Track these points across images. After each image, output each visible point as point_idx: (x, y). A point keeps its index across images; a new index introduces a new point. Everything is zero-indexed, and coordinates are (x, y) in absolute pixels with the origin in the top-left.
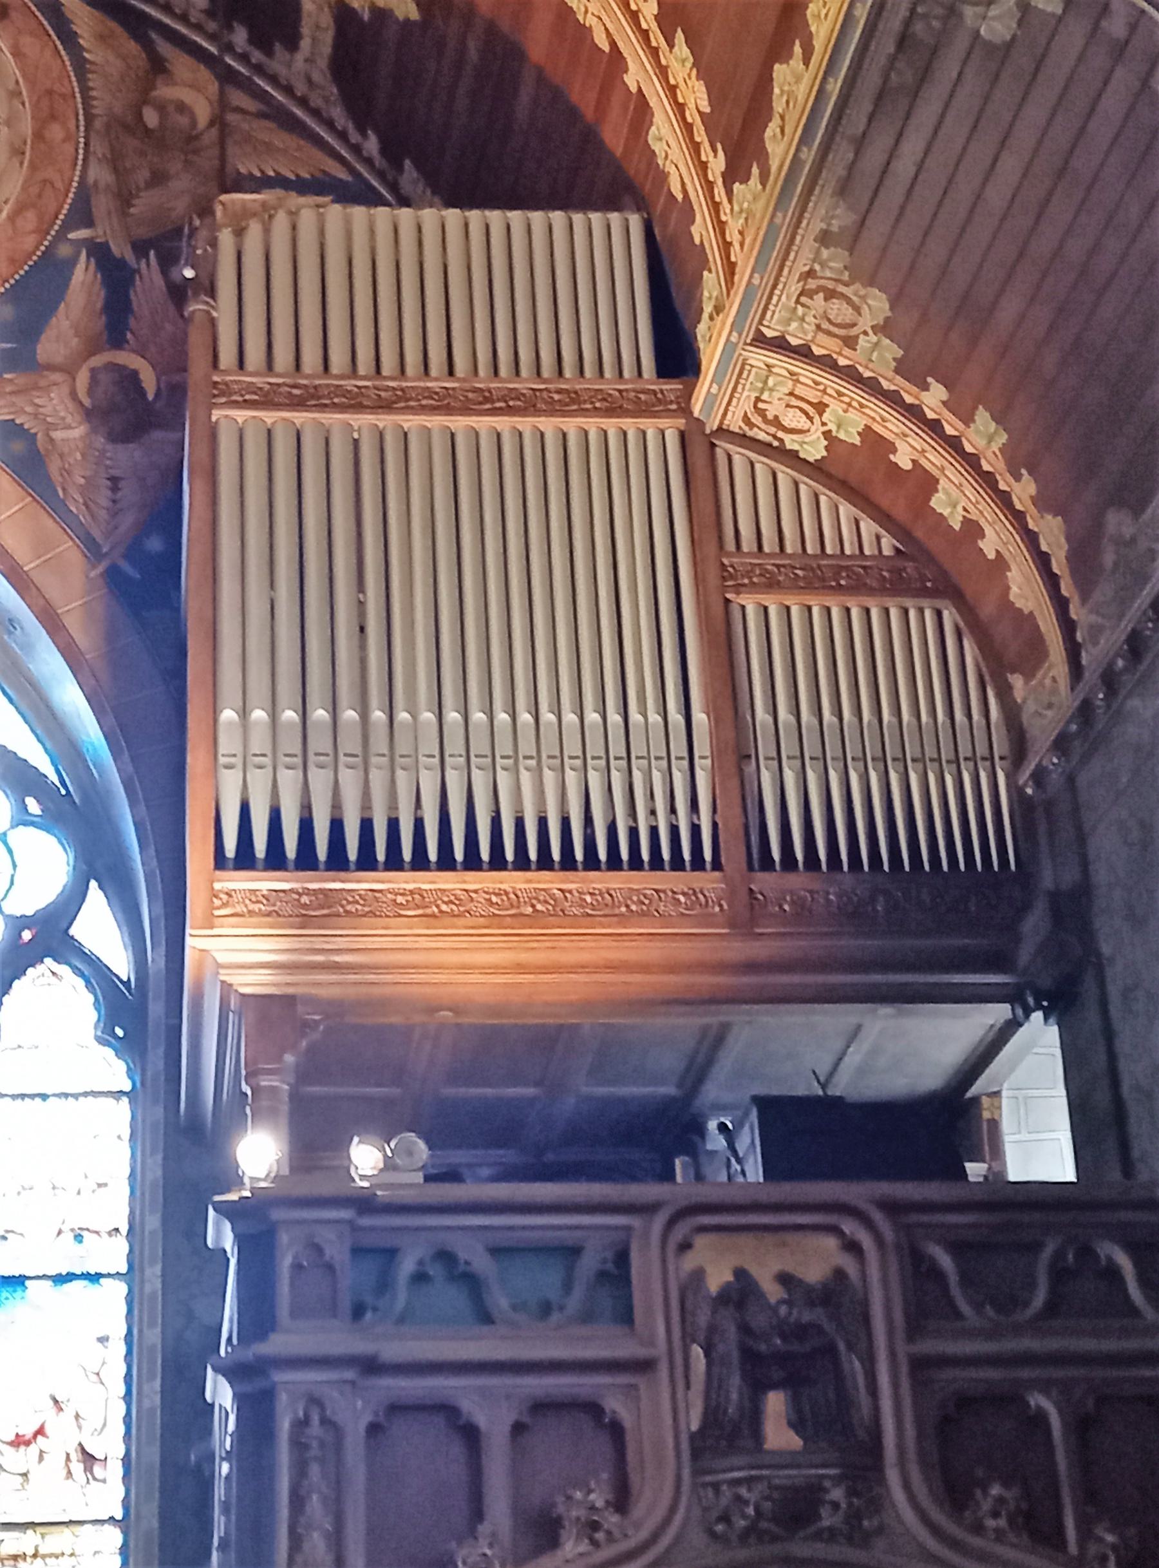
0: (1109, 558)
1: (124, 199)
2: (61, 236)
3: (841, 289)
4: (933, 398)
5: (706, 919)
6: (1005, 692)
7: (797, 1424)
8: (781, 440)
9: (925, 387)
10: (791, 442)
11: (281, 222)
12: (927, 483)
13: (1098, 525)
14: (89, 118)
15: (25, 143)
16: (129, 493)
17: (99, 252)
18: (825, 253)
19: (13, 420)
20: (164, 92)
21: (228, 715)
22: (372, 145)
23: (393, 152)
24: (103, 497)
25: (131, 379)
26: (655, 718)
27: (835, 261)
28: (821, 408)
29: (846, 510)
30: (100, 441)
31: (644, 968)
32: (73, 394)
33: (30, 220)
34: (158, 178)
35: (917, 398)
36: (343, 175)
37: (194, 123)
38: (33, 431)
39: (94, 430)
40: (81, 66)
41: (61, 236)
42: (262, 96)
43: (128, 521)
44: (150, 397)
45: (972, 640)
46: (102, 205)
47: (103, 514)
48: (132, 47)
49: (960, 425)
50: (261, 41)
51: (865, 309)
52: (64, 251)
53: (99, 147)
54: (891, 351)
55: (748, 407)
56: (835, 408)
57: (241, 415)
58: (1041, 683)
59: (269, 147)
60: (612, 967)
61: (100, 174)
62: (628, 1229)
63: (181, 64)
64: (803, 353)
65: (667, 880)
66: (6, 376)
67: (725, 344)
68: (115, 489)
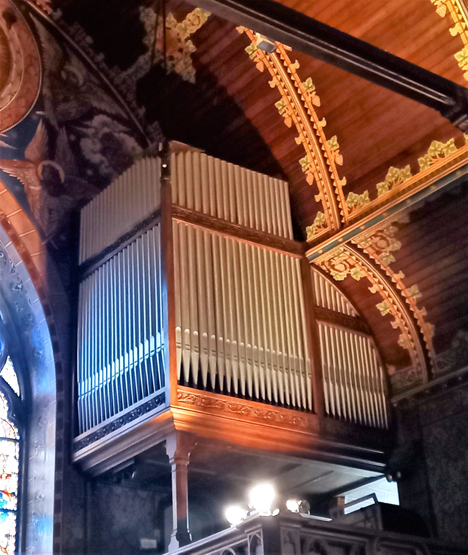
0: (455, 344)
1: (55, 104)
3: (388, 238)
6: (385, 370)
8: (330, 272)
9: (396, 272)
10: (333, 273)
11: (188, 154)
12: (378, 298)
13: (453, 333)
14: (44, 70)
15: (22, 72)
16: (55, 216)
18: (391, 227)
19: (16, 178)
21: (178, 329)
22: (142, 111)
24: (46, 215)
25: (55, 173)
26: (295, 357)
27: (393, 229)
28: (352, 267)
29: (343, 298)
30: (45, 194)
32: (37, 173)
33: (23, 102)
34: (66, 100)
35: (391, 275)
36: (125, 116)
37: (78, 82)
38: (23, 183)
39: (43, 189)
42: (101, 80)
43: (54, 227)
44: (63, 180)
45: (377, 351)
46: (48, 104)
47: (46, 223)
48: (58, 47)
49: (403, 287)
50: (110, 62)
51: (391, 246)
52: (34, 118)
53: (47, 80)
54: (392, 259)
55: (327, 259)
56: (358, 268)
57: (179, 221)
58: (406, 372)
59: (102, 100)
60: (259, 436)
61: (46, 91)
62: (364, 543)
63: (74, 60)
64: (360, 251)
66: (15, 160)
67: (336, 241)
68: (50, 213)
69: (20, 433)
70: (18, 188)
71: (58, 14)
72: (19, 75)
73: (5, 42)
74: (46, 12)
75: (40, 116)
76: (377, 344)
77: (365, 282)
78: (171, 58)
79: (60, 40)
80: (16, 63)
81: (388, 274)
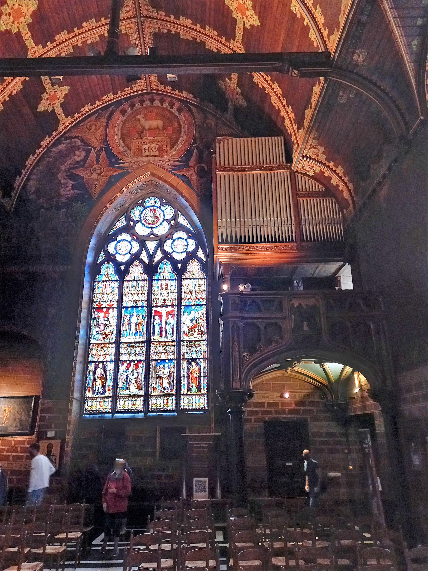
2: (192, 146)
4: (331, 164)
5: (295, 250)
7: (308, 327)
9: (330, 163)
10: (308, 173)
11: (226, 141)
12: (330, 178)
17: (197, 147)
20: (208, 121)
21: (219, 220)
23: (243, 129)
25: (204, 167)
26: (286, 218)
27: (315, 142)
28: (313, 167)
29: (317, 184)
30: (198, 178)
31: (284, 258)
32: (195, 171)
33: (187, 143)
40: (194, 118)
41: (192, 146)
42: (222, 121)
51: (320, 150)
54: (325, 157)
56: (315, 167)
57: (220, 173)
60: (279, 258)
62: (282, 297)
64: (310, 158)
65: (287, 244)
69: (206, 275)
70: (186, 179)
71: (198, 100)
72: (185, 132)
73: (178, 121)
74: (194, 101)
75: (195, 147)
76: (337, 201)
77: (322, 172)
78: (237, 99)
79: (203, 111)
80: (183, 128)
81: (327, 165)
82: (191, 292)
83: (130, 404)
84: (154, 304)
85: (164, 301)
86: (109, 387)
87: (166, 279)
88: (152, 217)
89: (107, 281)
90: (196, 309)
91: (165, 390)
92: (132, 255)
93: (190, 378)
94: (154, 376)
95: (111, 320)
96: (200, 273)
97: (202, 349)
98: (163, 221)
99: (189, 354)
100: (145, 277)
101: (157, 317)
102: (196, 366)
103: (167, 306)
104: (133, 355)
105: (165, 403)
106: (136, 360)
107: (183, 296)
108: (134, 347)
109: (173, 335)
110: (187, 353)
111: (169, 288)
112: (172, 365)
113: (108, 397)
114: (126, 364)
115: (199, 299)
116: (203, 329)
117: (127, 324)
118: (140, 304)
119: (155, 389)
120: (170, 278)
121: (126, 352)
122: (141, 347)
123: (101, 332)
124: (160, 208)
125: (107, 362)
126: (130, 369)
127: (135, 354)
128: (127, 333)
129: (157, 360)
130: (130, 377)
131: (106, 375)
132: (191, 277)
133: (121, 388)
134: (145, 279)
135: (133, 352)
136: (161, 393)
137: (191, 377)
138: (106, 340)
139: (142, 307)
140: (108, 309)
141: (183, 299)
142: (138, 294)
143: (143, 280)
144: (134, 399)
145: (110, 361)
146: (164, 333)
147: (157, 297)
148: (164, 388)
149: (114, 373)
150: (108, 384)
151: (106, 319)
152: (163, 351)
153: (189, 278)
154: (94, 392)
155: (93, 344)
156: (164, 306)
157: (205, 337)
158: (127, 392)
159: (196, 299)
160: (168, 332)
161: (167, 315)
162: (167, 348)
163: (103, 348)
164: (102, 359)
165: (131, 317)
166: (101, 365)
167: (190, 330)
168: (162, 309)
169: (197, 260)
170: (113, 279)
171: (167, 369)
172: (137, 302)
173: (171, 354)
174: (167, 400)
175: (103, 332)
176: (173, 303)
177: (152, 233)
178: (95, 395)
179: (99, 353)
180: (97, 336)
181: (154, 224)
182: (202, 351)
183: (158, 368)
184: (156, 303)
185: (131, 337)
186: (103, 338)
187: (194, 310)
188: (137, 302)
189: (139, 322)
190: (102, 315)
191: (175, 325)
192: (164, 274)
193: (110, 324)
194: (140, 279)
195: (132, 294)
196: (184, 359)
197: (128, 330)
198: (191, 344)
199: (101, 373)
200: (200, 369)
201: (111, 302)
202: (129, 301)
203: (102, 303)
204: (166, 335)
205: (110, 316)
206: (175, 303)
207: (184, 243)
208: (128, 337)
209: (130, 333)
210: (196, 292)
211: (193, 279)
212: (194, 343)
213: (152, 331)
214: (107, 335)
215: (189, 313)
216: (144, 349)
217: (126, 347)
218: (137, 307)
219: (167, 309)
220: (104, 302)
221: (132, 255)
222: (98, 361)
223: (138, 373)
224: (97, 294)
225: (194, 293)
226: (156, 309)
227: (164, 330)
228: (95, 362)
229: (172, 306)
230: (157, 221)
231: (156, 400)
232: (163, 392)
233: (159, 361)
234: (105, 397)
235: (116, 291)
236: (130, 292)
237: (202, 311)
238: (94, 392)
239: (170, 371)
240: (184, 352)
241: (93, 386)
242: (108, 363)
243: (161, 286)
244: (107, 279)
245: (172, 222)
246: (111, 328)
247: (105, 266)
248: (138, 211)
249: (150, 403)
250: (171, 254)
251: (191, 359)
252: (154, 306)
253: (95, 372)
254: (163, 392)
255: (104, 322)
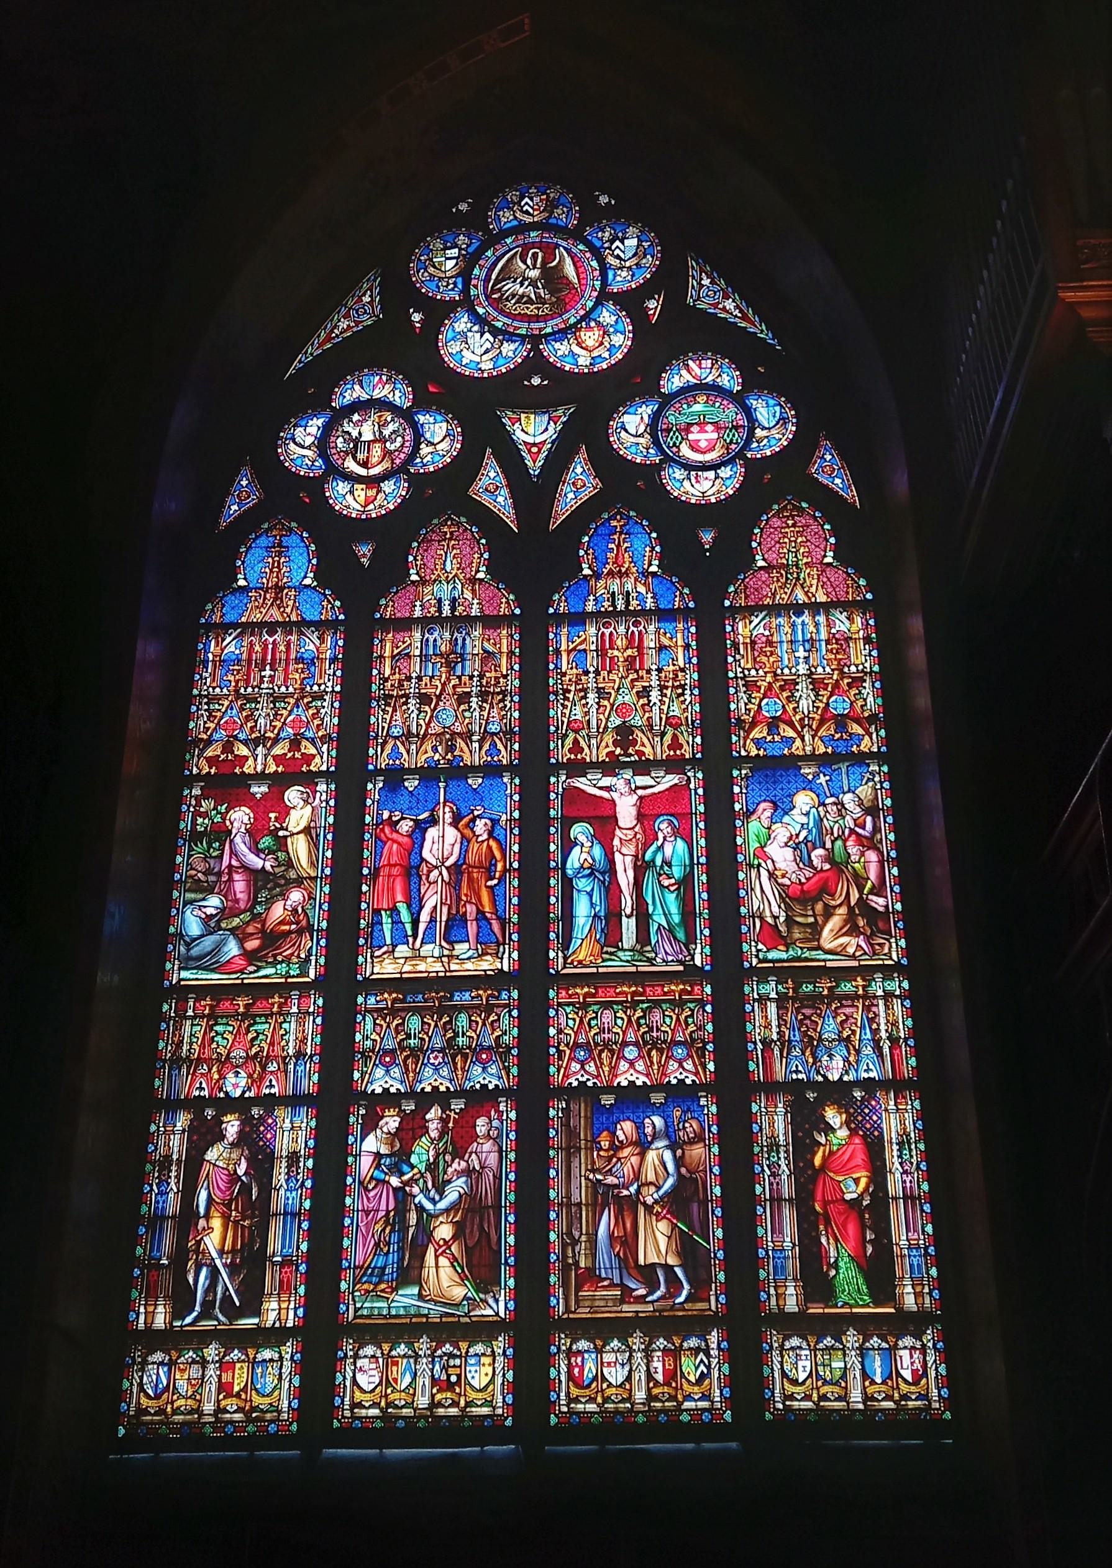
82: (790, 685)
83: (424, 1381)
84: (561, 752)
85: (625, 735)
86: (287, 1262)
87: (627, 613)
88: (533, 283)
89: (272, 627)
90: (822, 779)
91: (653, 1286)
92: (418, 482)
93: (818, 1208)
94: (580, 1194)
95: (300, 847)
96: (837, 576)
97: (883, 1021)
98: (599, 303)
99: (796, 1052)
100: (506, 604)
101: (580, 831)
102: (853, 1132)
103: (643, 767)
104: (435, 1059)
105: (660, 1377)
106: (460, 1093)
107: (740, 705)
108: (441, 1011)
109: (691, 938)
110: (786, 1044)
111: (651, 660)
112: (692, 1127)
113: (275, 1336)
114: (391, 1122)
115: (841, 722)
116: (878, 902)
117: (395, 871)
118: (472, 754)
119: (591, 1276)
120: (649, 604)
121: (390, 1044)
122: (489, 1009)
123: (236, 921)
124: (576, 235)
125: (270, 1102)
126: (422, 1153)
127: (451, 1050)
128: (397, 922)
129: (597, 1091)
130: (420, 1198)
131: (267, 1188)
132: (782, 598)
133: (362, 1271)
134: (504, 610)
135: (438, 1042)
136: (629, 1309)
137: (825, 1204)
138: (270, 971)
139: (491, 771)
140: (279, 782)
141: (740, 721)
142: (464, 698)
143: (491, 622)
144: (448, 1348)
145: (294, 1101)
146: (629, 927)
147: (578, 713)
148: (648, 1274)
149: (314, 1173)
150: (275, 1244)
151: (266, 842)
152: (631, 1037)
153: (768, 601)
154: (182, 1301)
155: (182, 992)
156: (626, 765)
157: (894, 949)
158: (405, 1299)
159: (822, 722)
160: (659, 918)
161: (640, 817)
162: (656, 1016)
163: (249, 1016)
164: (236, 1084)
165: (421, 828)
166: (232, 1127)
167: (798, 908)
168: (606, 781)
169: (814, 506)
170: (311, 615)
171: (659, 1155)
172: (460, 743)
173: (680, 1052)
174: (674, 1354)
175: (246, 917)
176: (675, 744)
177: (536, 362)
178: (188, 1320)
179: (222, 1045)
180: (209, 942)
181: (545, 319)
182: (884, 1035)
183: (605, 1144)
184: (576, 748)
185: (427, 949)
186: (250, 957)
187: (809, 785)
188: (460, 743)
189: (471, 858)
190: (240, 817)
191: (701, 878)
192: (615, 585)
193: (292, 875)
194: (475, 611)
195: (424, 699)
196: (771, 1088)
197: (402, 908)
198: (807, 988)
199: (233, 1178)
200: (875, 1148)
201: (295, 744)
202: (408, 735)
203: (243, 751)
204: (643, 935)
205: (299, 818)
206: (691, 744)
207: (730, 413)
208: (402, 950)
209: (415, 923)
210: (817, 685)
211: (798, 609)
212: (824, 986)
213: (556, 911)
214: (272, 939)
215: (781, 808)
216: (508, 1028)
217: (393, 1012)
218: (458, 772)
219: (641, 780)
220: (257, 742)
221: (418, 482)
222: (212, 1101)
223: (468, 1172)
224: (212, 699)
225: (803, 689)
226: (581, 783)
227: (628, 903)
228: (196, 1105)
229: (673, 765)
230: (560, 307)
231: (599, 1351)
232: (641, 1300)
233: (608, 1100)
234: (259, 1330)
235: (329, 680)
236: (411, 688)
237: (865, 791)
238: (182, 1301)
239: (679, 1162)
240: (767, 1043)
241: (180, 1257)
242: (279, 1112)
243: (602, 652)
244: (276, 615)
245: (653, 305)
246: (296, 896)
247: (263, 541)
248: (454, 252)
249: (559, 1371)
250: (651, 473)
251: (811, 1084)
252: (559, 766)
253: (194, 1163)
254: (641, 1300)
255: (256, 862)
